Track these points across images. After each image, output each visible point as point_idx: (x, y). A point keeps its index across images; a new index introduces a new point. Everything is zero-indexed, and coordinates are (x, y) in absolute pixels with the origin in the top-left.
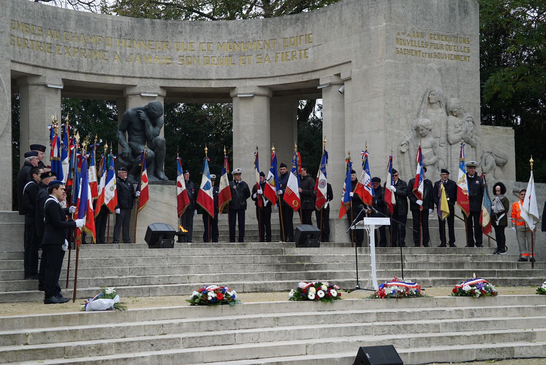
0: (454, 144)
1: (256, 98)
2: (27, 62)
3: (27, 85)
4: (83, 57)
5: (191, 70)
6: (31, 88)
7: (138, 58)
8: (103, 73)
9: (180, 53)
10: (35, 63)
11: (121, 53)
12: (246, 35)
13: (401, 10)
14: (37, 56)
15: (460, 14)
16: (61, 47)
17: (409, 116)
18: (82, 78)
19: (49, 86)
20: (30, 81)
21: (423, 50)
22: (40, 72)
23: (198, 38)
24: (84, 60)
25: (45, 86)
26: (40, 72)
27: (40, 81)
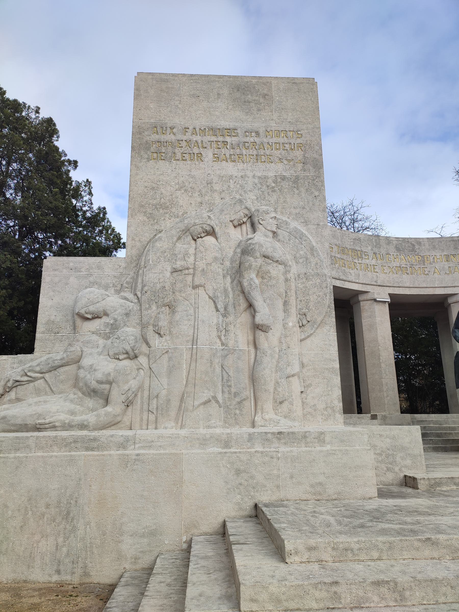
2: (357, 281)
3: (359, 302)
4: (406, 274)
6: (362, 303)
8: (425, 286)
10: (364, 282)
16: (385, 267)
19: (378, 300)
20: (361, 298)
25: (375, 300)
27: (369, 296)
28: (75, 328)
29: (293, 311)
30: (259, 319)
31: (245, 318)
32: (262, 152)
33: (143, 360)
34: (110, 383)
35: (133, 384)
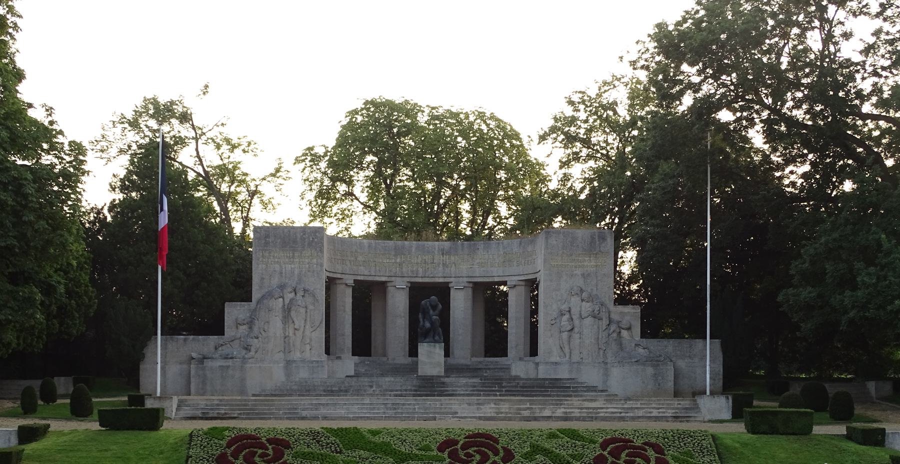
0: (585, 318)
1: (517, 287)
3: (388, 287)
5: (484, 271)
6: (389, 288)
7: (453, 266)
9: (478, 261)
11: (443, 263)
12: (512, 249)
13: (555, 242)
14: (391, 271)
15: (599, 241)
17: (559, 303)
18: (420, 280)
20: (389, 284)
21: (570, 264)
22: (393, 279)
23: (488, 252)
24: (420, 270)
26: (393, 279)
27: (393, 284)
28: (237, 328)
29: (308, 322)
30: (296, 327)
31: (291, 326)
32: (301, 260)
33: (260, 339)
34: (251, 346)
35: (258, 346)
